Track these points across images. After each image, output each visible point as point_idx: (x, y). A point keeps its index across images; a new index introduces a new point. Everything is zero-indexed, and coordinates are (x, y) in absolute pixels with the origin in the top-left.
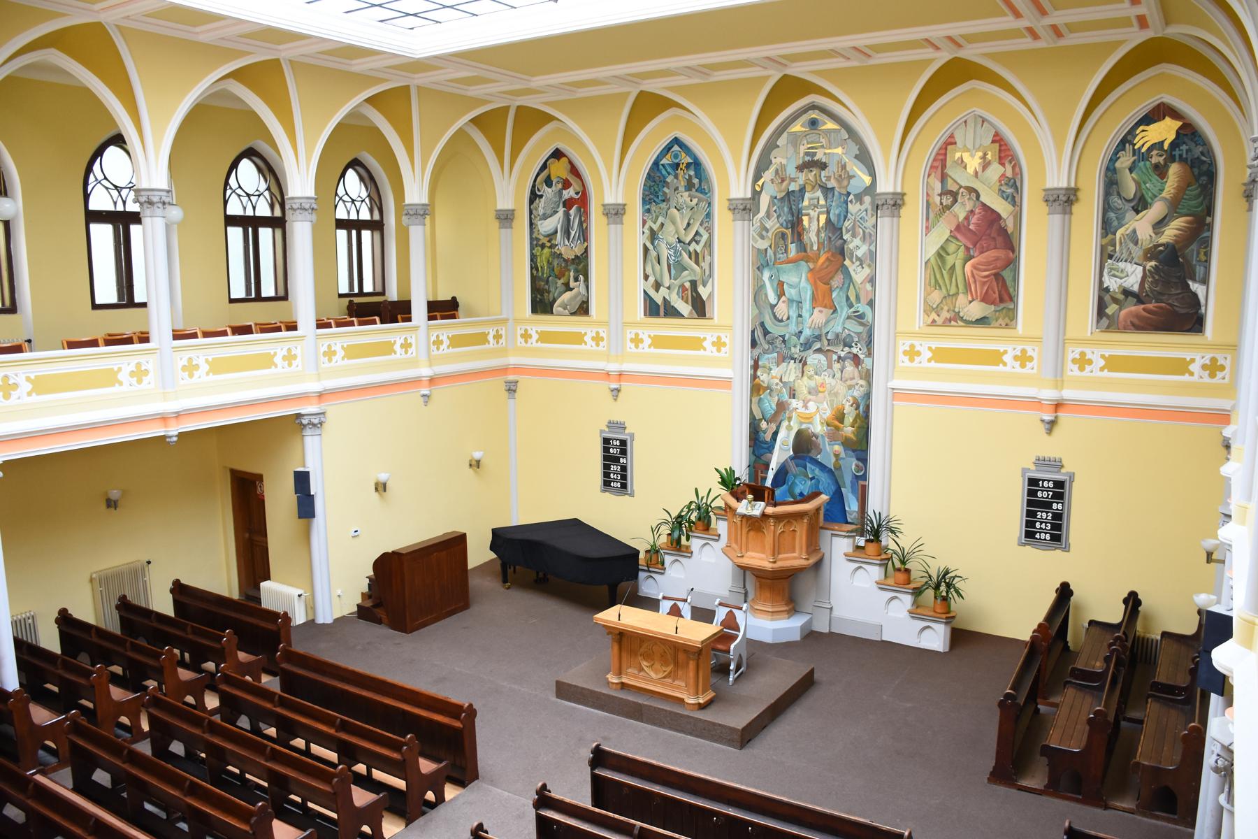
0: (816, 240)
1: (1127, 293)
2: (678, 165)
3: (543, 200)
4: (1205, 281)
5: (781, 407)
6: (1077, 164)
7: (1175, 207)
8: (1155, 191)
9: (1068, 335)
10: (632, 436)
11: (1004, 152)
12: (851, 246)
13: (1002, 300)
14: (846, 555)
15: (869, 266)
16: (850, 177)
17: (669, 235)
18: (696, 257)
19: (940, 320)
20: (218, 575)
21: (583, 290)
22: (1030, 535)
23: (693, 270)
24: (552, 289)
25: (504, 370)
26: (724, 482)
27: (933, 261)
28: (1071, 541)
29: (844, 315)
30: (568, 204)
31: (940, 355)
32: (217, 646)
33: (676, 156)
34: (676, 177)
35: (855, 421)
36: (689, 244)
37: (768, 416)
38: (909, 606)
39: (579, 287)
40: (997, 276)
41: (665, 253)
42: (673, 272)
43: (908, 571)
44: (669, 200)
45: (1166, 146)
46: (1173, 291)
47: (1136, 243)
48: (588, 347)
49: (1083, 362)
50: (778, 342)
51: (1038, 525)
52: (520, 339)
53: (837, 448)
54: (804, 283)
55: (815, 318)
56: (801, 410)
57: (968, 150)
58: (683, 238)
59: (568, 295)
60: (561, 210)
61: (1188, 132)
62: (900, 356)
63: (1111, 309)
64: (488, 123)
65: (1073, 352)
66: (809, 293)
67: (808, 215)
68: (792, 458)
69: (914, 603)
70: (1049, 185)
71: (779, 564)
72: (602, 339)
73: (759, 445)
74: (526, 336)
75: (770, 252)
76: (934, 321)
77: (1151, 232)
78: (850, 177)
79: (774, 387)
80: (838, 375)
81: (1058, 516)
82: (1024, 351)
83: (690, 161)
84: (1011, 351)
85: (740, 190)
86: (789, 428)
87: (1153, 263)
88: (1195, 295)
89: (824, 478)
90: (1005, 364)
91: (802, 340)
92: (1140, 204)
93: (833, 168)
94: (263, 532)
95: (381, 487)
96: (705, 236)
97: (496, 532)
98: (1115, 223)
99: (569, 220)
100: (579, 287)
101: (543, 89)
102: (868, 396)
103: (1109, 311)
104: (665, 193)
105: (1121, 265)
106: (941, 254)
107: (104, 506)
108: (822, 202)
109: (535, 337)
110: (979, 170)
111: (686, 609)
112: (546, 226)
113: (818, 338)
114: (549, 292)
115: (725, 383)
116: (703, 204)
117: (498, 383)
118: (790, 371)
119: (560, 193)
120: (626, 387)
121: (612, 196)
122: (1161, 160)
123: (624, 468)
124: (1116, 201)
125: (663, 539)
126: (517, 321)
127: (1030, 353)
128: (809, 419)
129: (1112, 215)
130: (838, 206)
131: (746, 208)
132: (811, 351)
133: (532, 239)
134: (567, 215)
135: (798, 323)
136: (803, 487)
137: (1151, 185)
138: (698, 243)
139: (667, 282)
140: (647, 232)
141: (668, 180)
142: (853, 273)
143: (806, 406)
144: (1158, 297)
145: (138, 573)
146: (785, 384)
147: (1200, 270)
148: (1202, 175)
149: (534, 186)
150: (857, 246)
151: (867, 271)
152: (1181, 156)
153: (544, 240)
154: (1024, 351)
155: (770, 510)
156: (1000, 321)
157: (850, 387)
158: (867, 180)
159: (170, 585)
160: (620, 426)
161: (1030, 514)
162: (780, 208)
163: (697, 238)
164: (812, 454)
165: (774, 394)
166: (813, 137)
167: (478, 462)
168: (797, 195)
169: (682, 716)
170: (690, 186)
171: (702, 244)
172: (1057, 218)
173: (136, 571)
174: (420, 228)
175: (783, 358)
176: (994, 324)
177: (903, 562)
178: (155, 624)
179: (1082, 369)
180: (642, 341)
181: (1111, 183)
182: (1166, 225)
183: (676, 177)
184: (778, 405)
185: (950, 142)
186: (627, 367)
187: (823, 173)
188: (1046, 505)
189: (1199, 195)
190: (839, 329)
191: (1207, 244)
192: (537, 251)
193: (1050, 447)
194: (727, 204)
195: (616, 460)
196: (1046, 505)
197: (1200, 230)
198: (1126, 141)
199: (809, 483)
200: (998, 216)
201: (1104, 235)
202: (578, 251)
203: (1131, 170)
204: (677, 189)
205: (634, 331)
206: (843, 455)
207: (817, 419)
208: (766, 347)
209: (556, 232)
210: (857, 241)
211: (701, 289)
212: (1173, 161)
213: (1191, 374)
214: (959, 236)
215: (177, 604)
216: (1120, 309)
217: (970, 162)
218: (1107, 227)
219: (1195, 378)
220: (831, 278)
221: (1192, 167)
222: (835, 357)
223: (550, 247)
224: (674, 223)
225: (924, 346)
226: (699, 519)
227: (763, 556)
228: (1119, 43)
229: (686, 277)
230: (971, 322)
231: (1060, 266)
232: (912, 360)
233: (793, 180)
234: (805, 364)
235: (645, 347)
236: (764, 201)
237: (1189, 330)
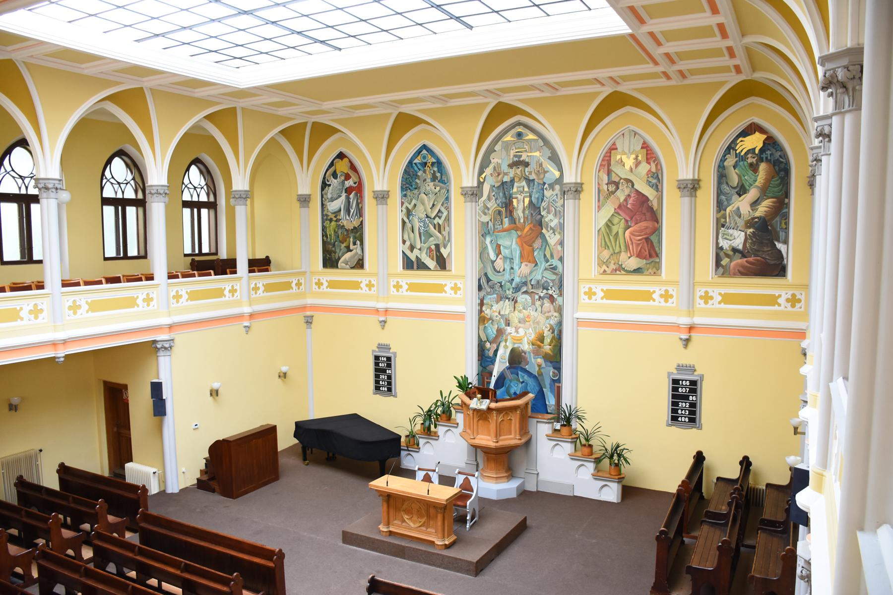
0: (522, 216)
1: (735, 250)
2: (426, 163)
3: (331, 188)
4: (786, 242)
5: (500, 332)
6: (699, 164)
7: (764, 192)
8: (751, 181)
9: (697, 279)
11: (650, 155)
12: (546, 220)
13: (651, 256)
14: (547, 436)
15: (559, 233)
16: (545, 172)
17: (420, 212)
18: (439, 228)
19: (608, 271)
20: (94, 459)
21: (359, 251)
22: (674, 419)
23: (437, 238)
24: (338, 251)
25: (303, 308)
26: (460, 386)
27: (603, 229)
28: (703, 421)
29: (543, 267)
30: (349, 191)
31: (609, 295)
32: (92, 511)
33: (424, 158)
34: (425, 172)
35: (551, 341)
39: (356, 249)
40: (647, 240)
41: (417, 225)
42: (423, 238)
43: (590, 446)
45: (757, 151)
46: (766, 249)
47: (740, 217)
48: (363, 291)
49: (707, 298)
50: (497, 286)
51: (679, 411)
52: (314, 286)
53: (540, 360)
54: (514, 246)
55: (523, 270)
56: (514, 334)
57: (625, 154)
58: (429, 215)
59: (348, 255)
60: (344, 195)
61: (771, 142)
62: (582, 296)
64: (292, 133)
65: (700, 292)
66: (518, 252)
68: (508, 368)
69: (596, 468)
70: (680, 178)
71: (500, 443)
72: (373, 286)
73: (485, 359)
74: (319, 284)
75: (490, 224)
76: (605, 271)
78: (545, 172)
80: (539, 309)
81: (693, 405)
82: (666, 291)
83: (434, 161)
84: (658, 291)
85: (469, 180)
86: (506, 347)
87: (751, 230)
88: (780, 252)
89: (531, 382)
90: (654, 300)
91: (514, 285)
92: (742, 190)
93: (533, 166)
94: (128, 427)
95: (214, 393)
96: (445, 213)
97: (297, 423)
98: (725, 203)
99: (349, 202)
100: (356, 249)
101: (330, 110)
102: (560, 323)
105: (731, 231)
106: (609, 225)
107: (7, 407)
108: (526, 189)
109: (326, 284)
110: (633, 167)
111: (435, 477)
112: (333, 206)
113: (525, 284)
114: (335, 253)
115: (460, 316)
116: (443, 191)
117: (300, 317)
118: (506, 307)
119: (343, 183)
120: (390, 319)
121: (379, 186)
122: (754, 160)
123: (389, 377)
124: (725, 188)
125: (418, 427)
126: (313, 273)
127: (671, 292)
128: (520, 340)
129: (723, 197)
130: (537, 192)
131: (473, 194)
132: (520, 293)
133: (323, 215)
134: (348, 198)
136: (516, 388)
137: (748, 177)
138: (440, 218)
140: (405, 210)
141: (419, 174)
142: (548, 238)
143: (517, 332)
144: (755, 253)
145: (32, 459)
146: (502, 316)
147: (782, 235)
148: (781, 171)
149: (324, 178)
150: (551, 220)
151: (558, 237)
152: (767, 158)
153: (332, 216)
154: (666, 291)
155: (493, 405)
156: (650, 270)
157: (548, 318)
158: (557, 174)
159: (57, 467)
160: (387, 347)
161: (674, 404)
162: (498, 193)
163: (440, 214)
164: (522, 365)
165: (495, 323)
167: (285, 374)
168: (509, 184)
169: (434, 554)
170: (434, 178)
171: (443, 218)
172: (687, 200)
173: (31, 457)
174: (243, 207)
175: (501, 298)
177: (587, 440)
178: (45, 497)
179: (706, 303)
180: (401, 287)
181: (722, 176)
182: (759, 204)
183: (425, 172)
185: (613, 148)
186: (391, 305)
187: (527, 169)
188: (685, 397)
189: (780, 184)
190: (539, 278)
191: (786, 217)
192: (327, 223)
193: (687, 357)
194: (460, 190)
195: (384, 371)
196: (685, 397)
197: (781, 207)
198: (730, 148)
199: (520, 385)
200: (647, 199)
201: (719, 211)
202: (356, 223)
203: (735, 167)
204: (425, 180)
205: (396, 280)
206: (543, 365)
207: (525, 340)
208: (489, 290)
209: (340, 210)
210: (551, 216)
211: (442, 250)
212: (762, 161)
213: (779, 305)
214: (620, 212)
215: (62, 481)
216: (731, 261)
217: (627, 162)
218: (720, 206)
219: (782, 308)
220: (534, 242)
221: (774, 166)
222: (537, 297)
223: (336, 221)
224: (423, 204)
225: (598, 289)
226: (443, 412)
227: (489, 438)
228: (722, 84)
229: (432, 242)
230: (630, 272)
231: (690, 232)
232: (590, 298)
234: (516, 302)
236: (486, 188)
237: (777, 276)
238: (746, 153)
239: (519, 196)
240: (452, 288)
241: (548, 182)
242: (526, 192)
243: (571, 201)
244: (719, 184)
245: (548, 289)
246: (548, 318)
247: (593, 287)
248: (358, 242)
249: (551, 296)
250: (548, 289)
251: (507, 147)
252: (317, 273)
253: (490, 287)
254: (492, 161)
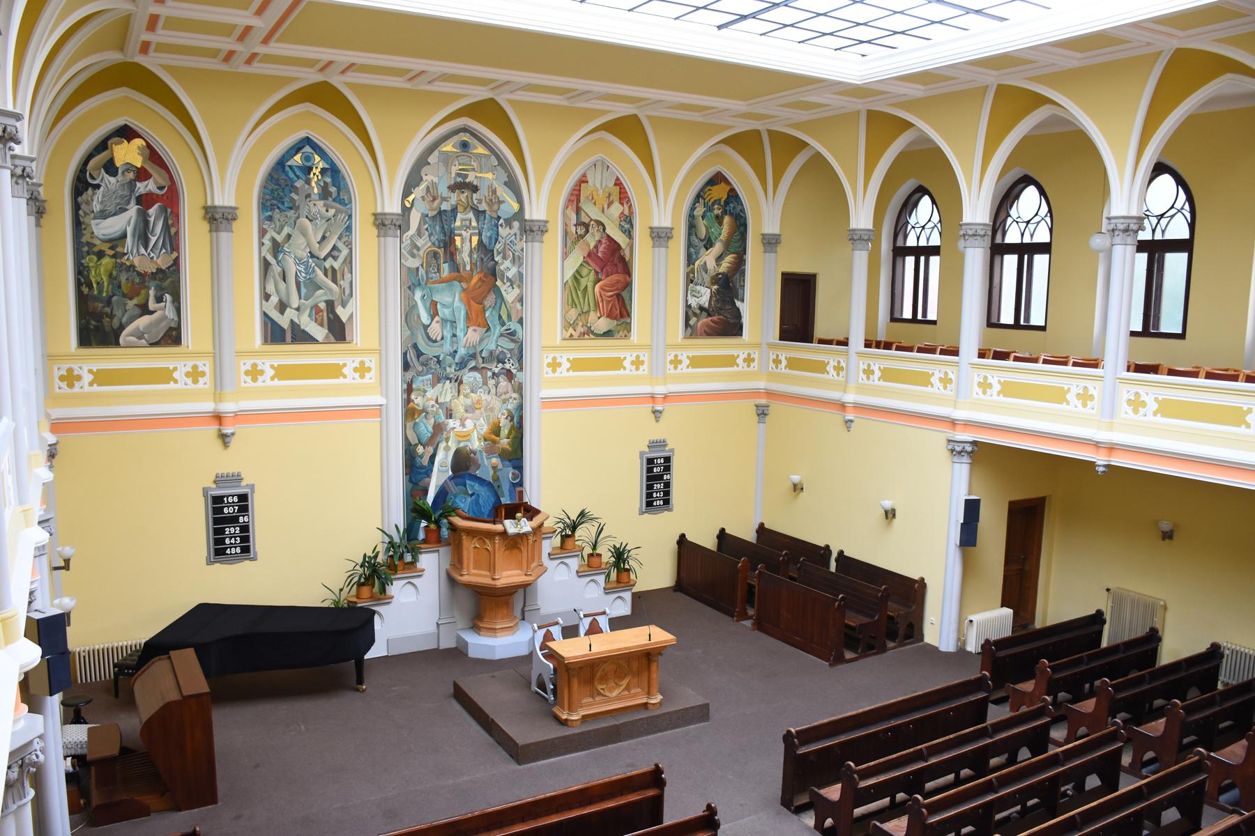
0: (466, 259)
1: (701, 308)
3: (100, 192)
5: (438, 428)
7: (727, 244)
10: (252, 487)
11: (623, 197)
12: (502, 267)
13: (622, 316)
15: (519, 286)
16: (500, 202)
17: (298, 248)
18: (334, 275)
19: (576, 335)
21: (170, 313)
22: (649, 504)
23: (330, 290)
24: (118, 313)
30: (145, 201)
31: (577, 365)
34: (308, 182)
35: (510, 432)
36: (325, 259)
37: (424, 440)
38: (603, 585)
40: (619, 296)
41: (292, 268)
42: (303, 291)
44: (298, 208)
49: (676, 362)
50: (433, 364)
53: (494, 460)
54: (457, 303)
55: (470, 337)
56: (459, 429)
58: (316, 253)
60: (133, 210)
61: (733, 195)
63: (693, 321)
67: (460, 235)
68: (451, 479)
73: (415, 470)
77: (714, 263)
78: (500, 202)
79: (430, 409)
80: (493, 391)
86: (447, 449)
89: (483, 492)
91: (457, 359)
92: (709, 244)
93: (483, 192)
99: (146, 223)
102: (520, 407)
103: (691, 322)
104: (293, 200)
105: (698, 288)
106: (577, 277)
108: (474, 224)
109: (740, 361)
111: (603, 622)
112: (105, 228)
113: (473, 356)
114: (111, 316)
115: (377, 411)
116: (341, 216)
118: (446, 392)
119: (131, 185)
121: (223, 198)
123: (245, 528)
124: (695, 240)
128: (467, 436)
130: (489, 229)
132: (466, 370)
135: (452, 343)
138: (335, 258)
139: (295, 302)
141: (299, 184)
142: (504, 293)
143: (463, 425)
144: (719, 311)
146: (441, 405)
147: (740, 291)
150: (507, 268)
151: (517, 291)
153: (105, 247)
157: (504, 401)
158: (516, 206)
160: (236, 479)
161: (649, 487)
163: (335, 253)
166: (464, 159)
168: (449, 214)
169: (657, 716)
171: (341, 259)
175: (438, 380)
176: (617, 336)
180: (262, 372)
181: (692, 227)
184: (434, 427)
185: (583, 180)
190: (492, 347)
191: (743, 273)
193: (657, 432)
195: (233, 520)
197: (739, 264)
198: (698, 197)
199: (469, 499)
202: (163, 261)
203: (703, 218)
204: (308, 196)
206: (500, 466)
207: (475, 434)
208: (420, 369)
209: (124, 236)
210: (507, 263)
211: (339, 310)
218: (690, 260)
220: (484, 298)
222: (490, 374)
223: (114, 256)
225: (564, 358)
227: (518, 572)
229: (320, 297)
232: (554, 371)
233: (444, 199)
234: (461, 382)
235: (683, 368)
238: (713, 204)
239: (464, 233)
240: (355, 370)
241: (504, 216)
242: (474, 228)
243: (536, 244)
244: (690, 234)
245: (504, 363)
247: (558, 356)
248: (168, 297)
249: (509, 371)
250: (504, 363)
251: (447, 159)
252: (253, 353)
253: (423, 364)
254: (425, 178)
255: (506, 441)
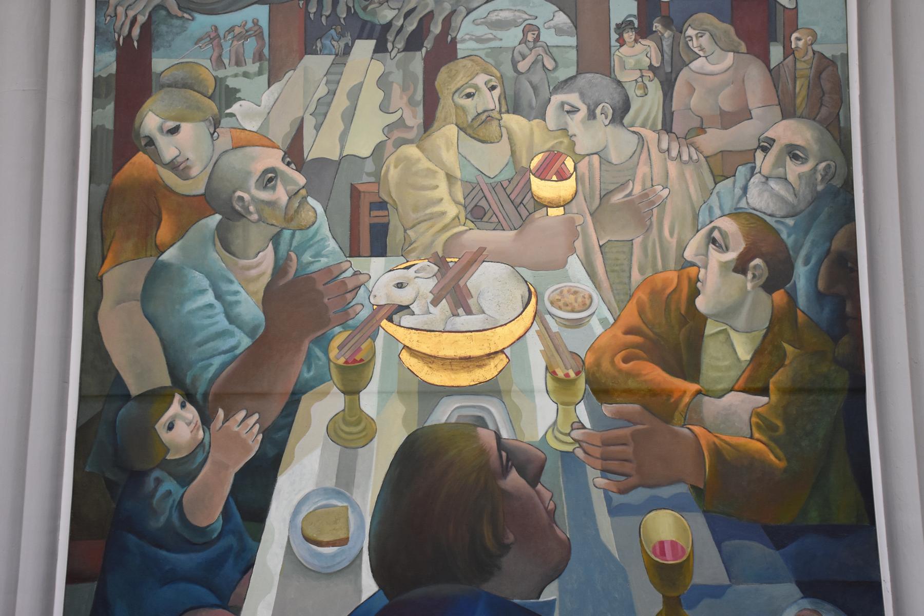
35: (767, 354)
37: (209, 370)
53: (664, 526)
79: (253, 193)
80: (647, 103)
86: (351, 431)
102: (834, 202)
143: (455, 294)
146: (320, 174)
157: (722, 167)
165: (255, 235)
184: (271, 297)
206: (709, 568)
234: (444, 53)
246: (722, 167)
255: (742, 404)
